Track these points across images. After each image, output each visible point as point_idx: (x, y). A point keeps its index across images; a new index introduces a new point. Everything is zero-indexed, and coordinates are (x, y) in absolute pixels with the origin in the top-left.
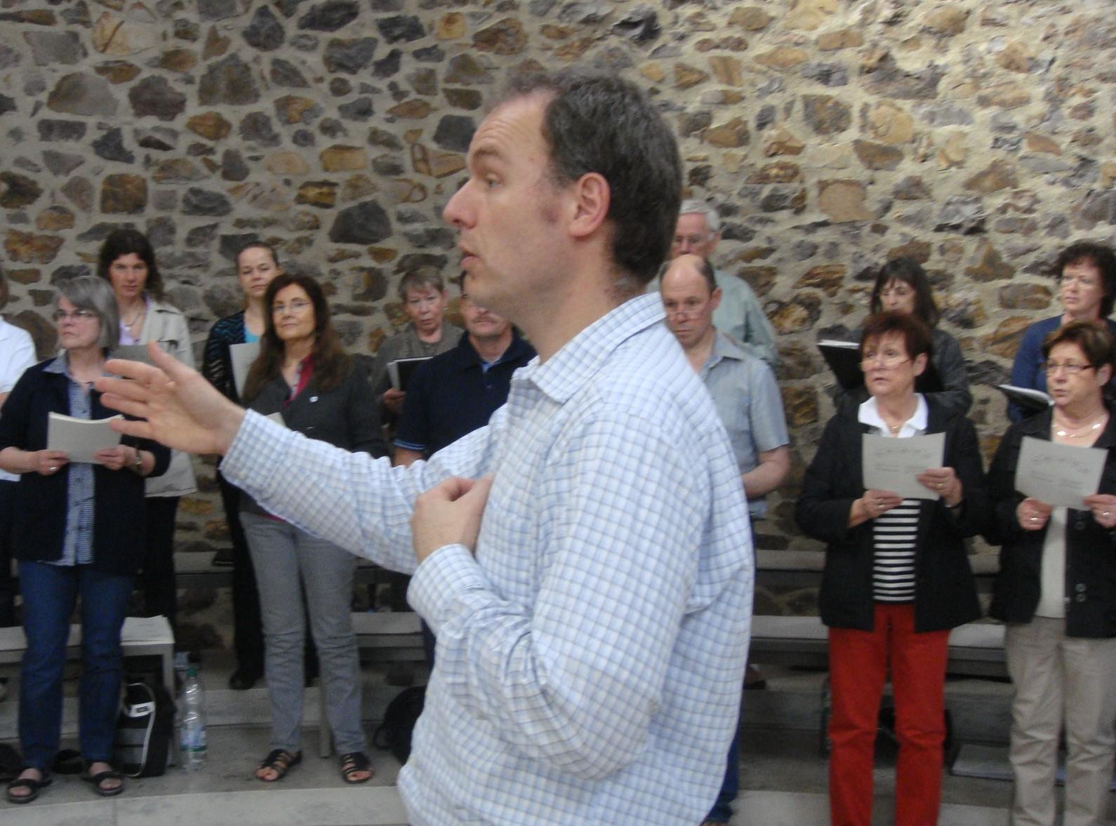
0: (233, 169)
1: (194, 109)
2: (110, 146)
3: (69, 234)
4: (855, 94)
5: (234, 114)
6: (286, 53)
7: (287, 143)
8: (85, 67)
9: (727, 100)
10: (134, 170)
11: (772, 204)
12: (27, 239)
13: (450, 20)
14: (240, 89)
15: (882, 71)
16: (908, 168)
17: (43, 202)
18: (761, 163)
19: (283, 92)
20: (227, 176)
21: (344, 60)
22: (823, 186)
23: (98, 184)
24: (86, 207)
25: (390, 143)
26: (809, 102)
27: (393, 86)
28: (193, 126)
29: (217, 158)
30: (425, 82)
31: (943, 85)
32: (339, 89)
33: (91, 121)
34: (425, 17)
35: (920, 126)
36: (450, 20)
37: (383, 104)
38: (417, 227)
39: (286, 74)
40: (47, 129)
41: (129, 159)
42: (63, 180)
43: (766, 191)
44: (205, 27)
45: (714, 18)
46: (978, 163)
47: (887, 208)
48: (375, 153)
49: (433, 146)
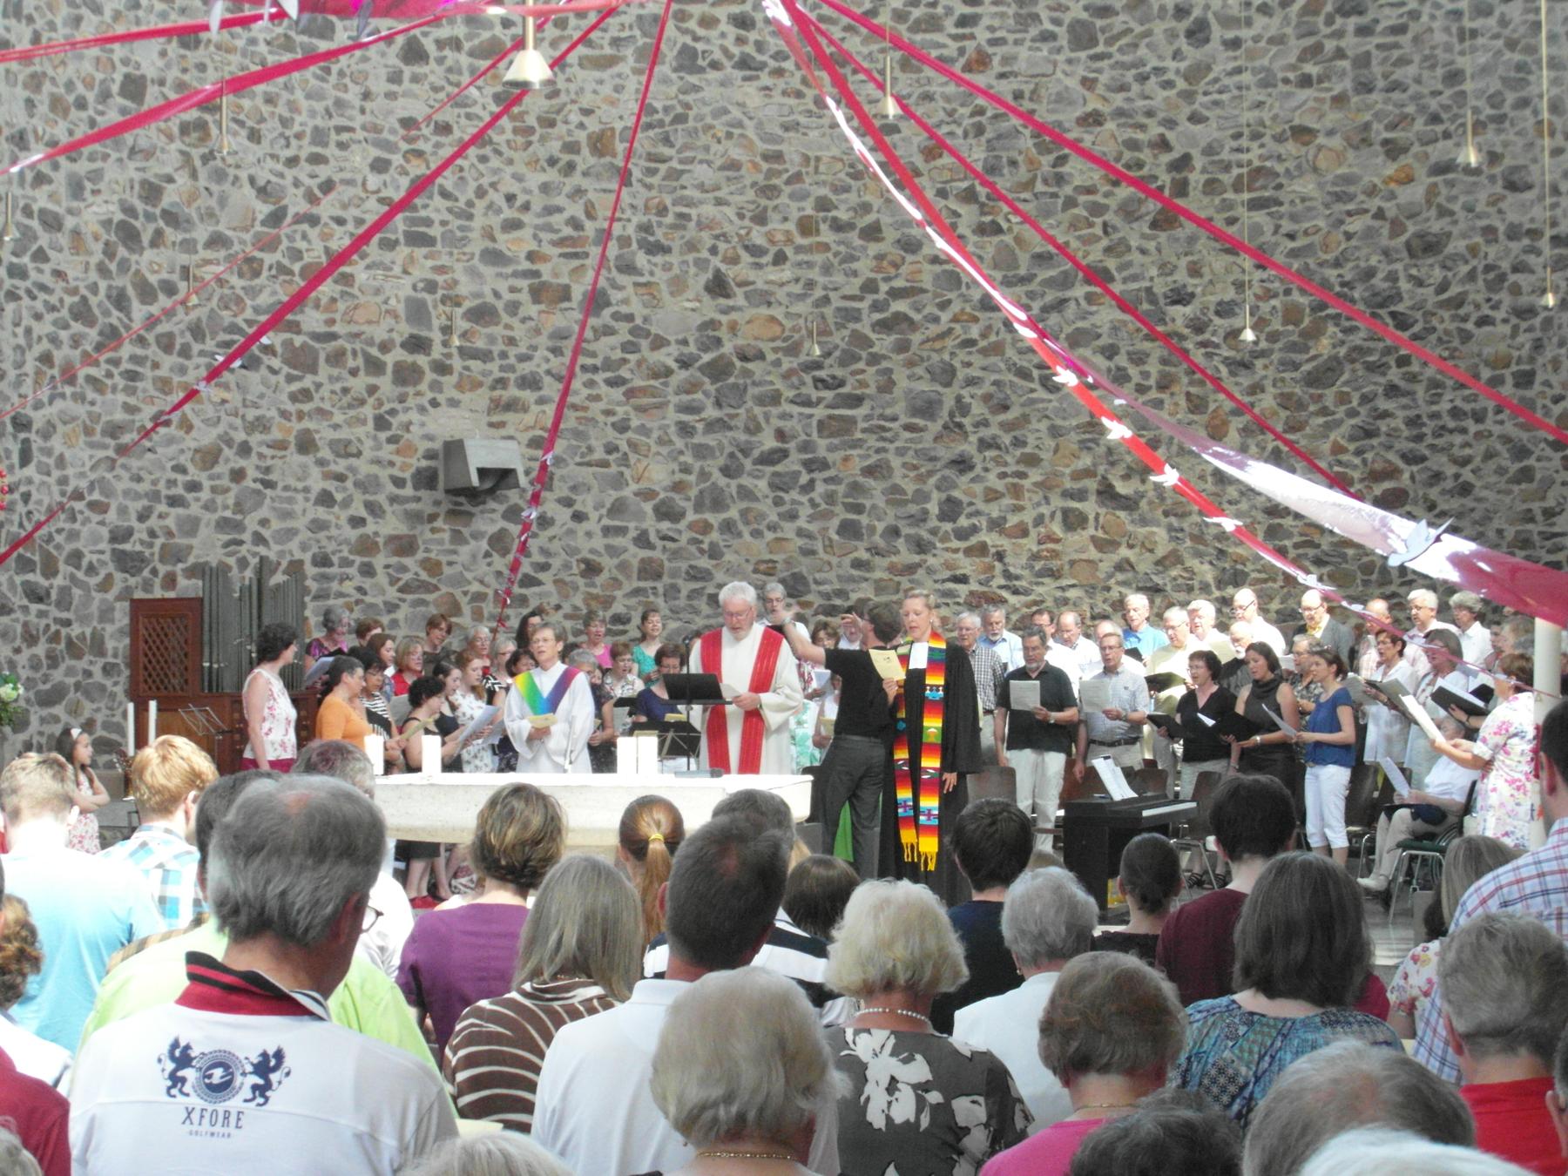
0: (714, 553)
1: (691, 516)
2: (642, 540)
3: (618, 594)
4: (1090, 507)
5: (714, 519)
6: (745, 481)
7: (747, 536)
8: (627, 492)
9: (1018, 509)
10: (656, 554)
11: (1040, 574)
12: (595, 597)
13: (846, 459)
14: (718, 504)
15: (1107, 493)
16: (1124, 552)
17: (605, 576)
18: (1035, 549)
19: (744, 505)
20: (711, 557)
21: (780, 485)
22: (1072, 563)
23: (635, 563)
24: (629, 577)
25: (810, 536)
26: (1066, 513)
27: (811, 501)
28: (691, 527)
29: (705, 546)
30: (830, 498)
31: (1143, 504)
32: (778, 502)
33: (632, 525)
34: (831, 457)
35: (1130, 528)
36: (846, 459)
37: (805, 511)
38: (826, 588)
39: (746, 494)
40: (607, 531)
41: (651, 546)
42: (616, 561)
43: (1038, 566)
44: (697, 465)
45: (1009, 459)
46: (1161, 552)
47: (1110, 576)
48: (800, 542)
49: (835, 537)
